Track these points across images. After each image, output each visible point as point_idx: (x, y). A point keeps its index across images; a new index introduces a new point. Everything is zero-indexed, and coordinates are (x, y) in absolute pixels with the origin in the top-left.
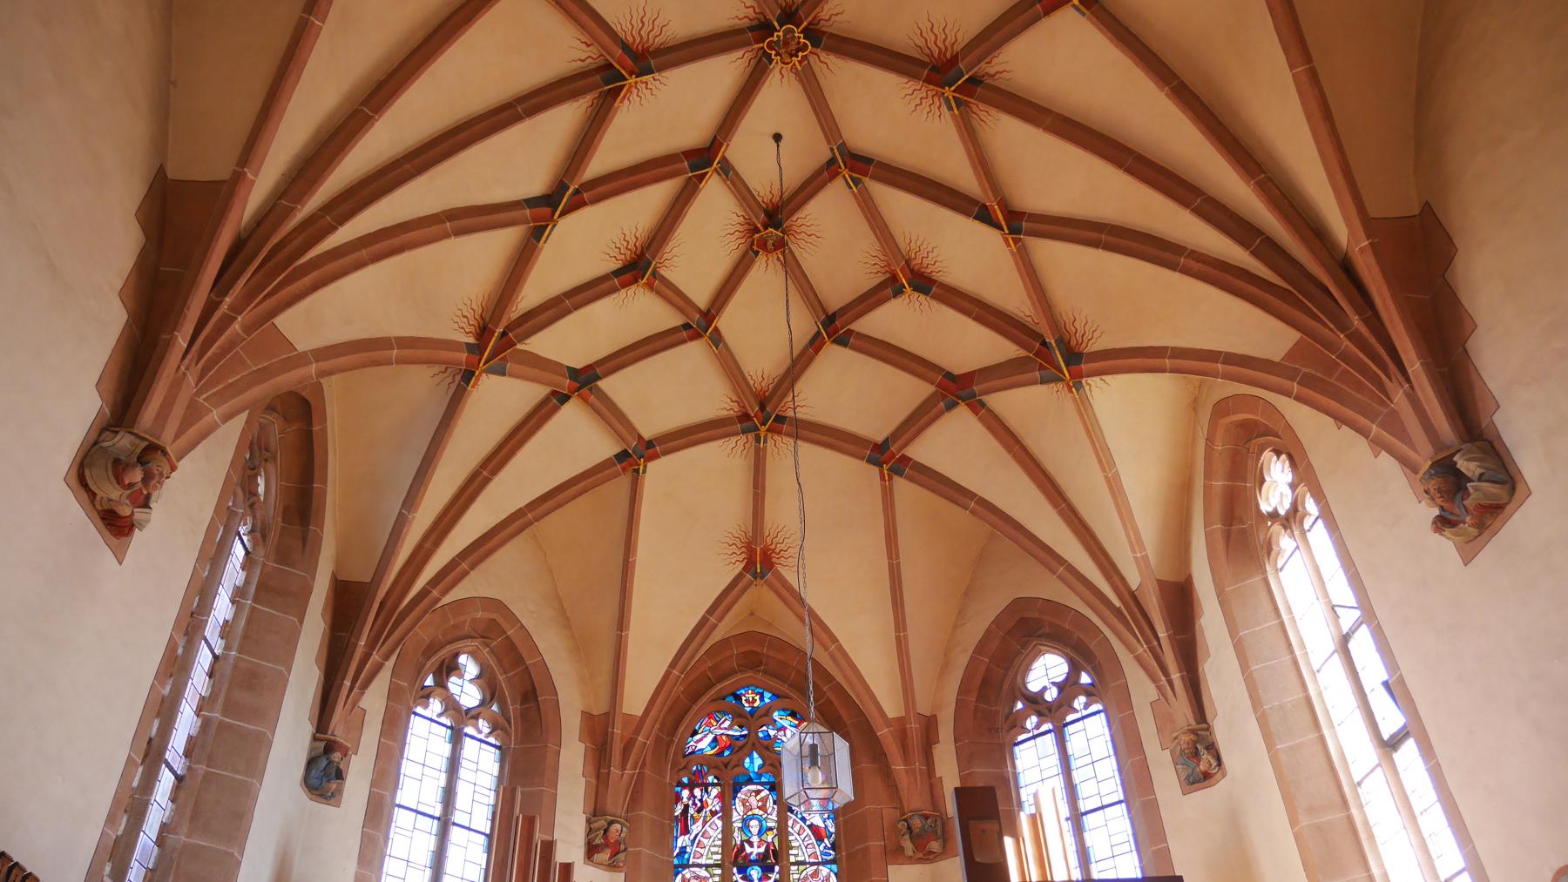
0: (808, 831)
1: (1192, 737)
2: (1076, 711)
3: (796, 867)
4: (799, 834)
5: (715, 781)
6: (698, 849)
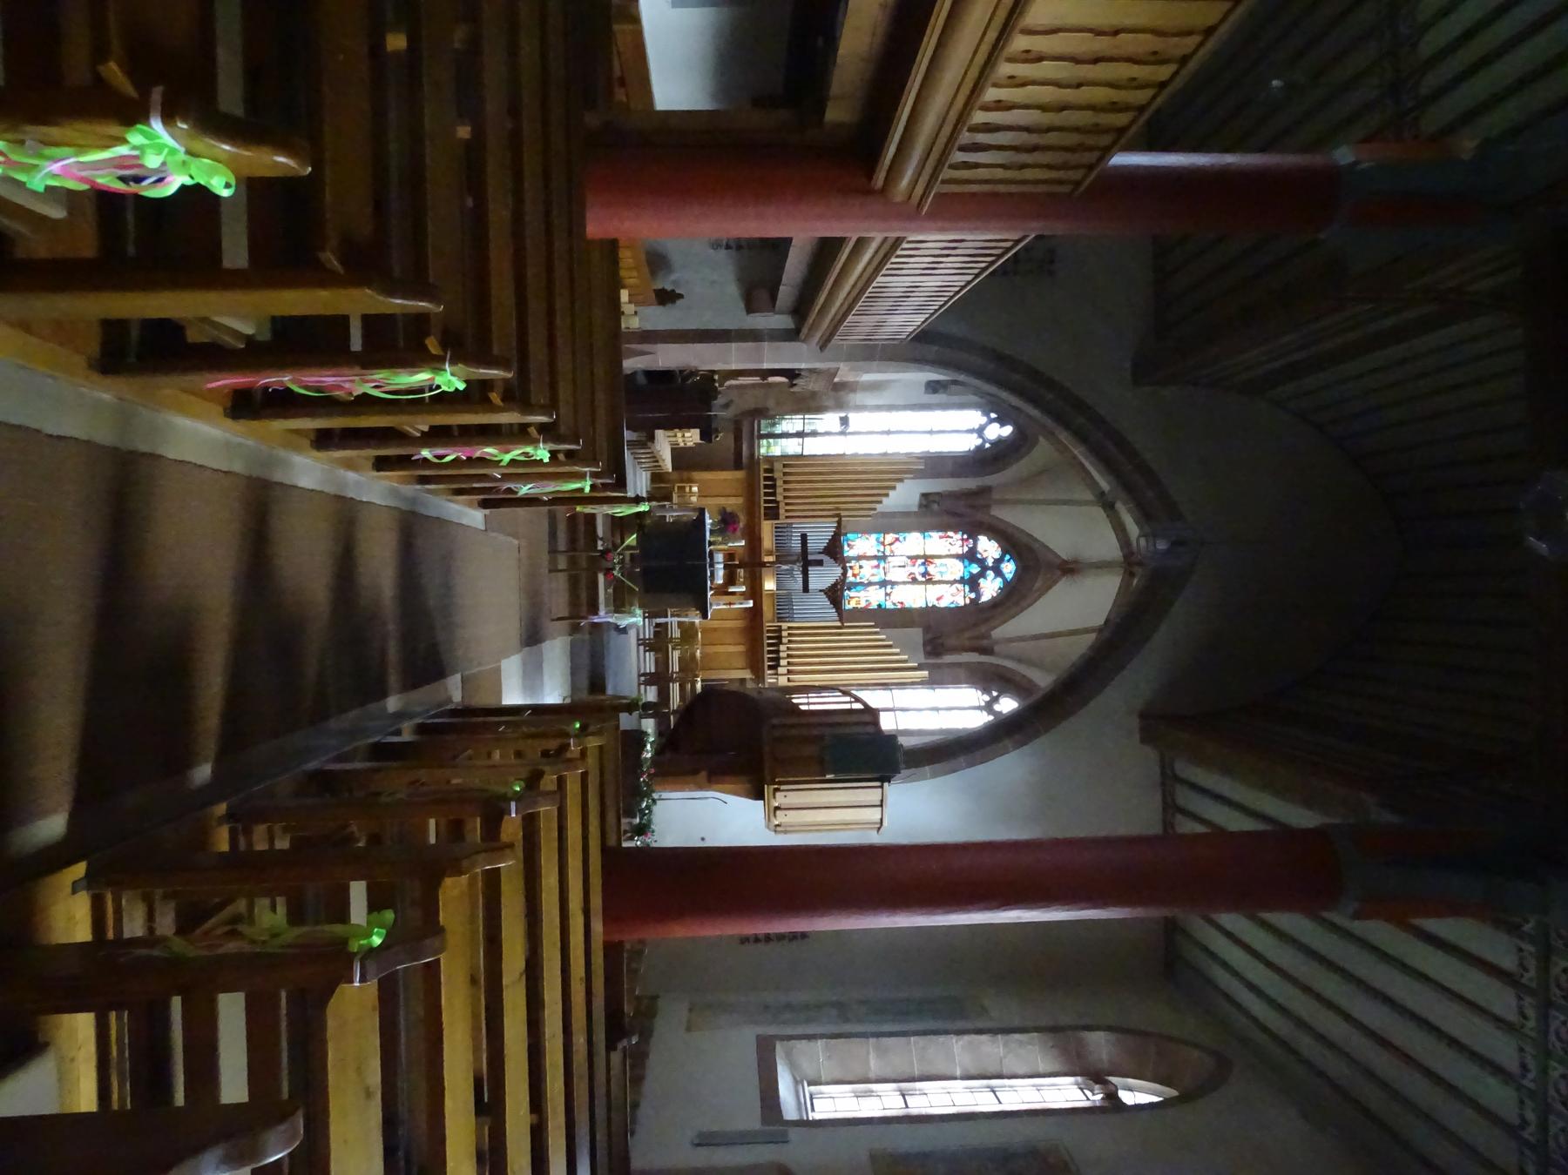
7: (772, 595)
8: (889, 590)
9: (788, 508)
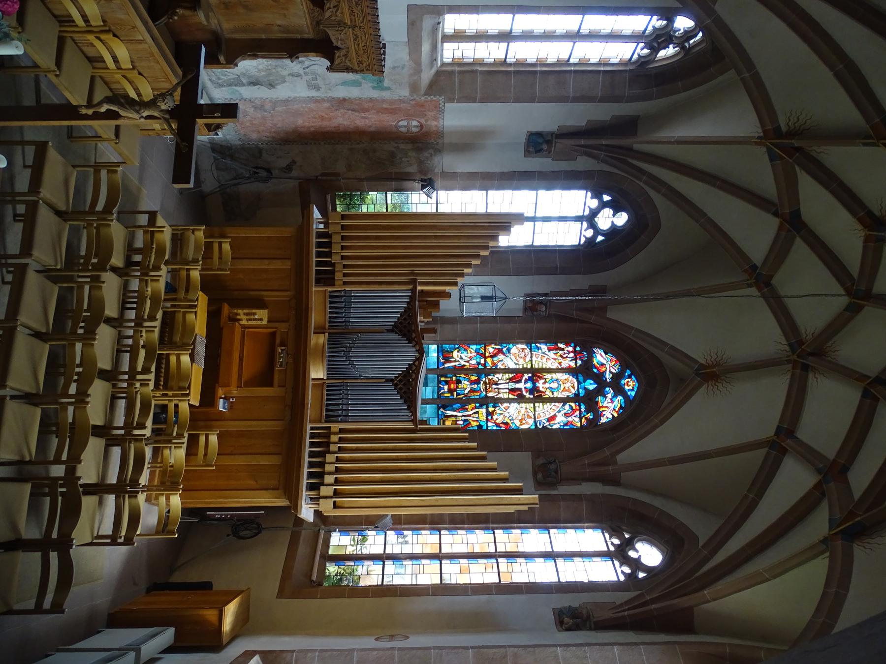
0: (552, 414)
1: (585, 616)
2: (621, 566)
3: (532, 407)
4: (551, 409)
5: (578, 365)
6: (540, 356)
7: (319, 384)
8: (491, 409)
9: (346, 271)
